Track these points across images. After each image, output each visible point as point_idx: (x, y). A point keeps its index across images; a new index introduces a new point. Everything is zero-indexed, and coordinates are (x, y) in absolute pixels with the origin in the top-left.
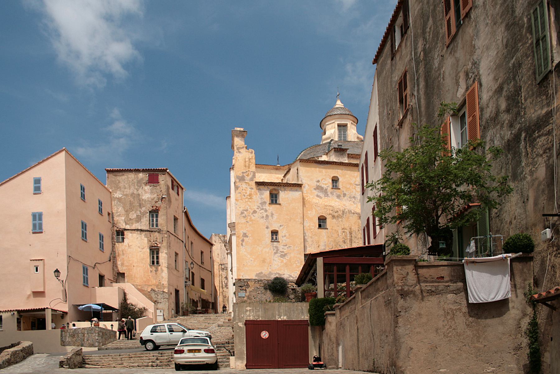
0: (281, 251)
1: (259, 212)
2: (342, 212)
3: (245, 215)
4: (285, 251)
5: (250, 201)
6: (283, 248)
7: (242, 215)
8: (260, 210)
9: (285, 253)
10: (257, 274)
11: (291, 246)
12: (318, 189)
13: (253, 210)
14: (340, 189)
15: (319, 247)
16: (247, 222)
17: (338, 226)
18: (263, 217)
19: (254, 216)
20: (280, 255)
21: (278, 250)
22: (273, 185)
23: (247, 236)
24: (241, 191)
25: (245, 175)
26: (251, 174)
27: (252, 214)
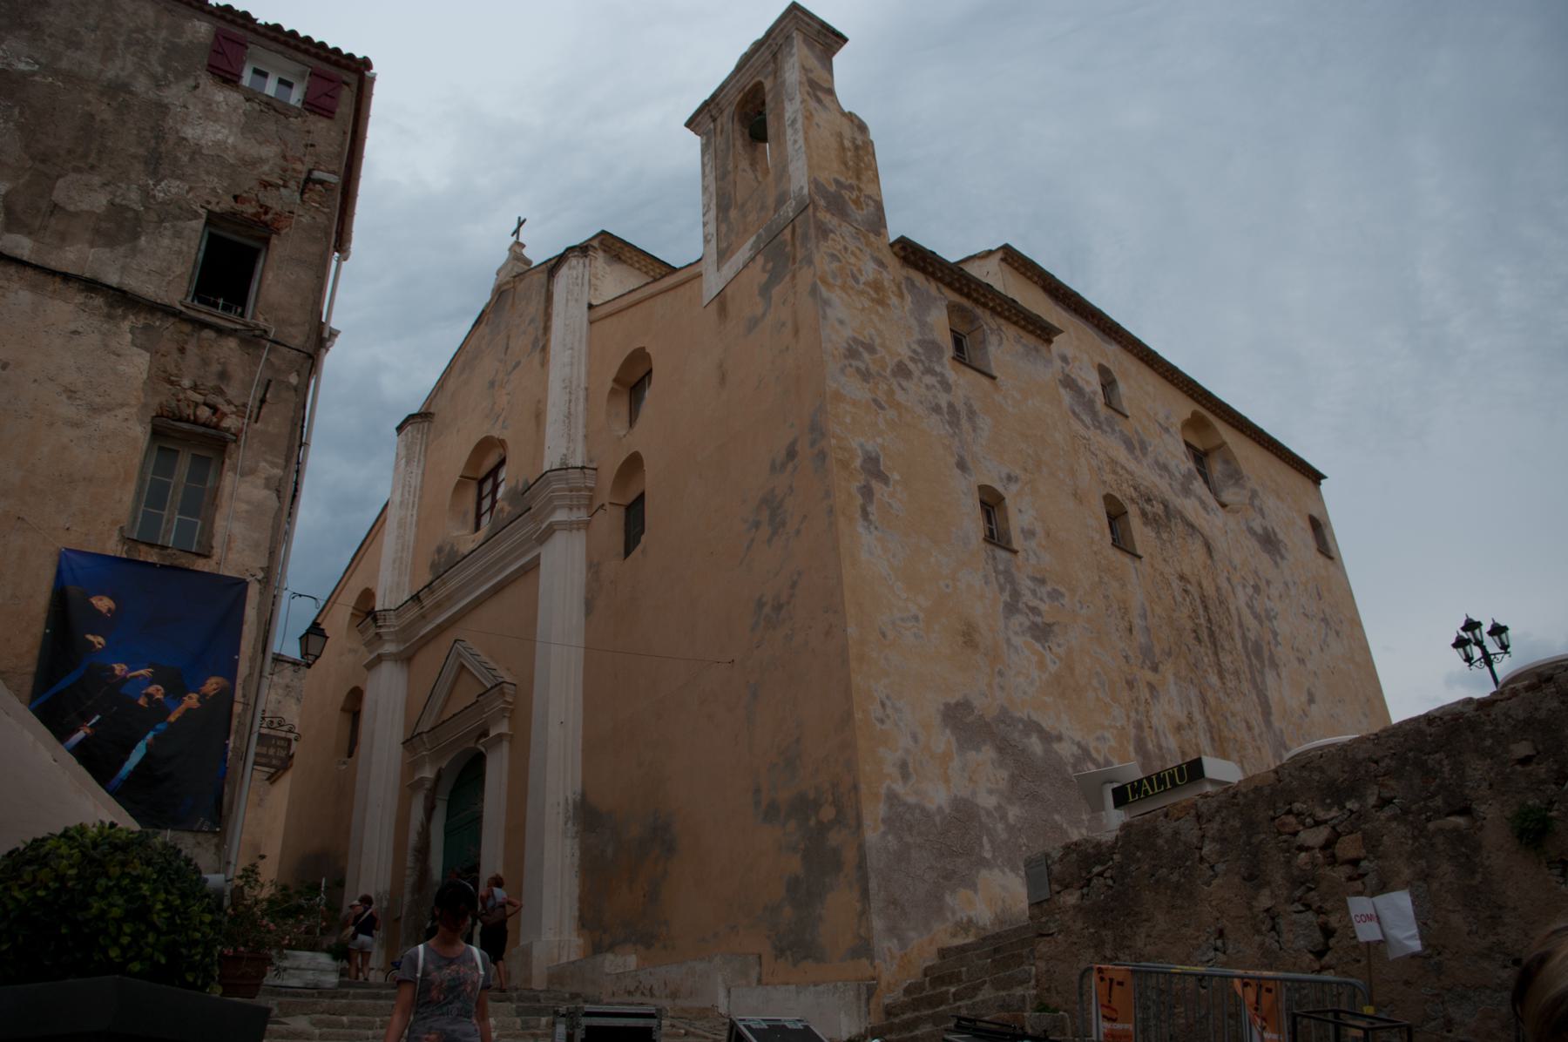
0: (1030, 604)
1: (920, 380)
2: (1161, 506)
3: (867, 369)
4: (1044, 607)
5: (877, 312)
6: (1034, 592)
7: (854, 363)
8: (923, 374)
9: (1049, 620)
10: (947, 705)
11: (1063, 590)
12: (1071, 389)
13: (896, 360)
14: (1127, 417)
15: (1131, 630)
16: (875, 401)
17: (1165, 560)
18: (937, 409)
19: (900, 385)
20: (1027, 623)
21: (1016, 594)
22: (959, 291)
23: (885, 480)
24: (840, 251)
25: (847, 198)
26: (867, 205)
27: (894, 374)
